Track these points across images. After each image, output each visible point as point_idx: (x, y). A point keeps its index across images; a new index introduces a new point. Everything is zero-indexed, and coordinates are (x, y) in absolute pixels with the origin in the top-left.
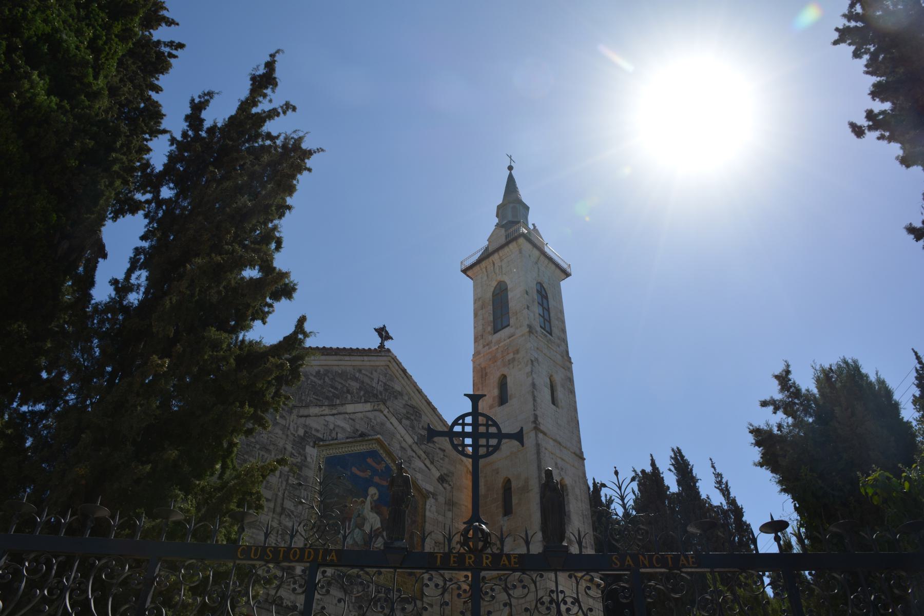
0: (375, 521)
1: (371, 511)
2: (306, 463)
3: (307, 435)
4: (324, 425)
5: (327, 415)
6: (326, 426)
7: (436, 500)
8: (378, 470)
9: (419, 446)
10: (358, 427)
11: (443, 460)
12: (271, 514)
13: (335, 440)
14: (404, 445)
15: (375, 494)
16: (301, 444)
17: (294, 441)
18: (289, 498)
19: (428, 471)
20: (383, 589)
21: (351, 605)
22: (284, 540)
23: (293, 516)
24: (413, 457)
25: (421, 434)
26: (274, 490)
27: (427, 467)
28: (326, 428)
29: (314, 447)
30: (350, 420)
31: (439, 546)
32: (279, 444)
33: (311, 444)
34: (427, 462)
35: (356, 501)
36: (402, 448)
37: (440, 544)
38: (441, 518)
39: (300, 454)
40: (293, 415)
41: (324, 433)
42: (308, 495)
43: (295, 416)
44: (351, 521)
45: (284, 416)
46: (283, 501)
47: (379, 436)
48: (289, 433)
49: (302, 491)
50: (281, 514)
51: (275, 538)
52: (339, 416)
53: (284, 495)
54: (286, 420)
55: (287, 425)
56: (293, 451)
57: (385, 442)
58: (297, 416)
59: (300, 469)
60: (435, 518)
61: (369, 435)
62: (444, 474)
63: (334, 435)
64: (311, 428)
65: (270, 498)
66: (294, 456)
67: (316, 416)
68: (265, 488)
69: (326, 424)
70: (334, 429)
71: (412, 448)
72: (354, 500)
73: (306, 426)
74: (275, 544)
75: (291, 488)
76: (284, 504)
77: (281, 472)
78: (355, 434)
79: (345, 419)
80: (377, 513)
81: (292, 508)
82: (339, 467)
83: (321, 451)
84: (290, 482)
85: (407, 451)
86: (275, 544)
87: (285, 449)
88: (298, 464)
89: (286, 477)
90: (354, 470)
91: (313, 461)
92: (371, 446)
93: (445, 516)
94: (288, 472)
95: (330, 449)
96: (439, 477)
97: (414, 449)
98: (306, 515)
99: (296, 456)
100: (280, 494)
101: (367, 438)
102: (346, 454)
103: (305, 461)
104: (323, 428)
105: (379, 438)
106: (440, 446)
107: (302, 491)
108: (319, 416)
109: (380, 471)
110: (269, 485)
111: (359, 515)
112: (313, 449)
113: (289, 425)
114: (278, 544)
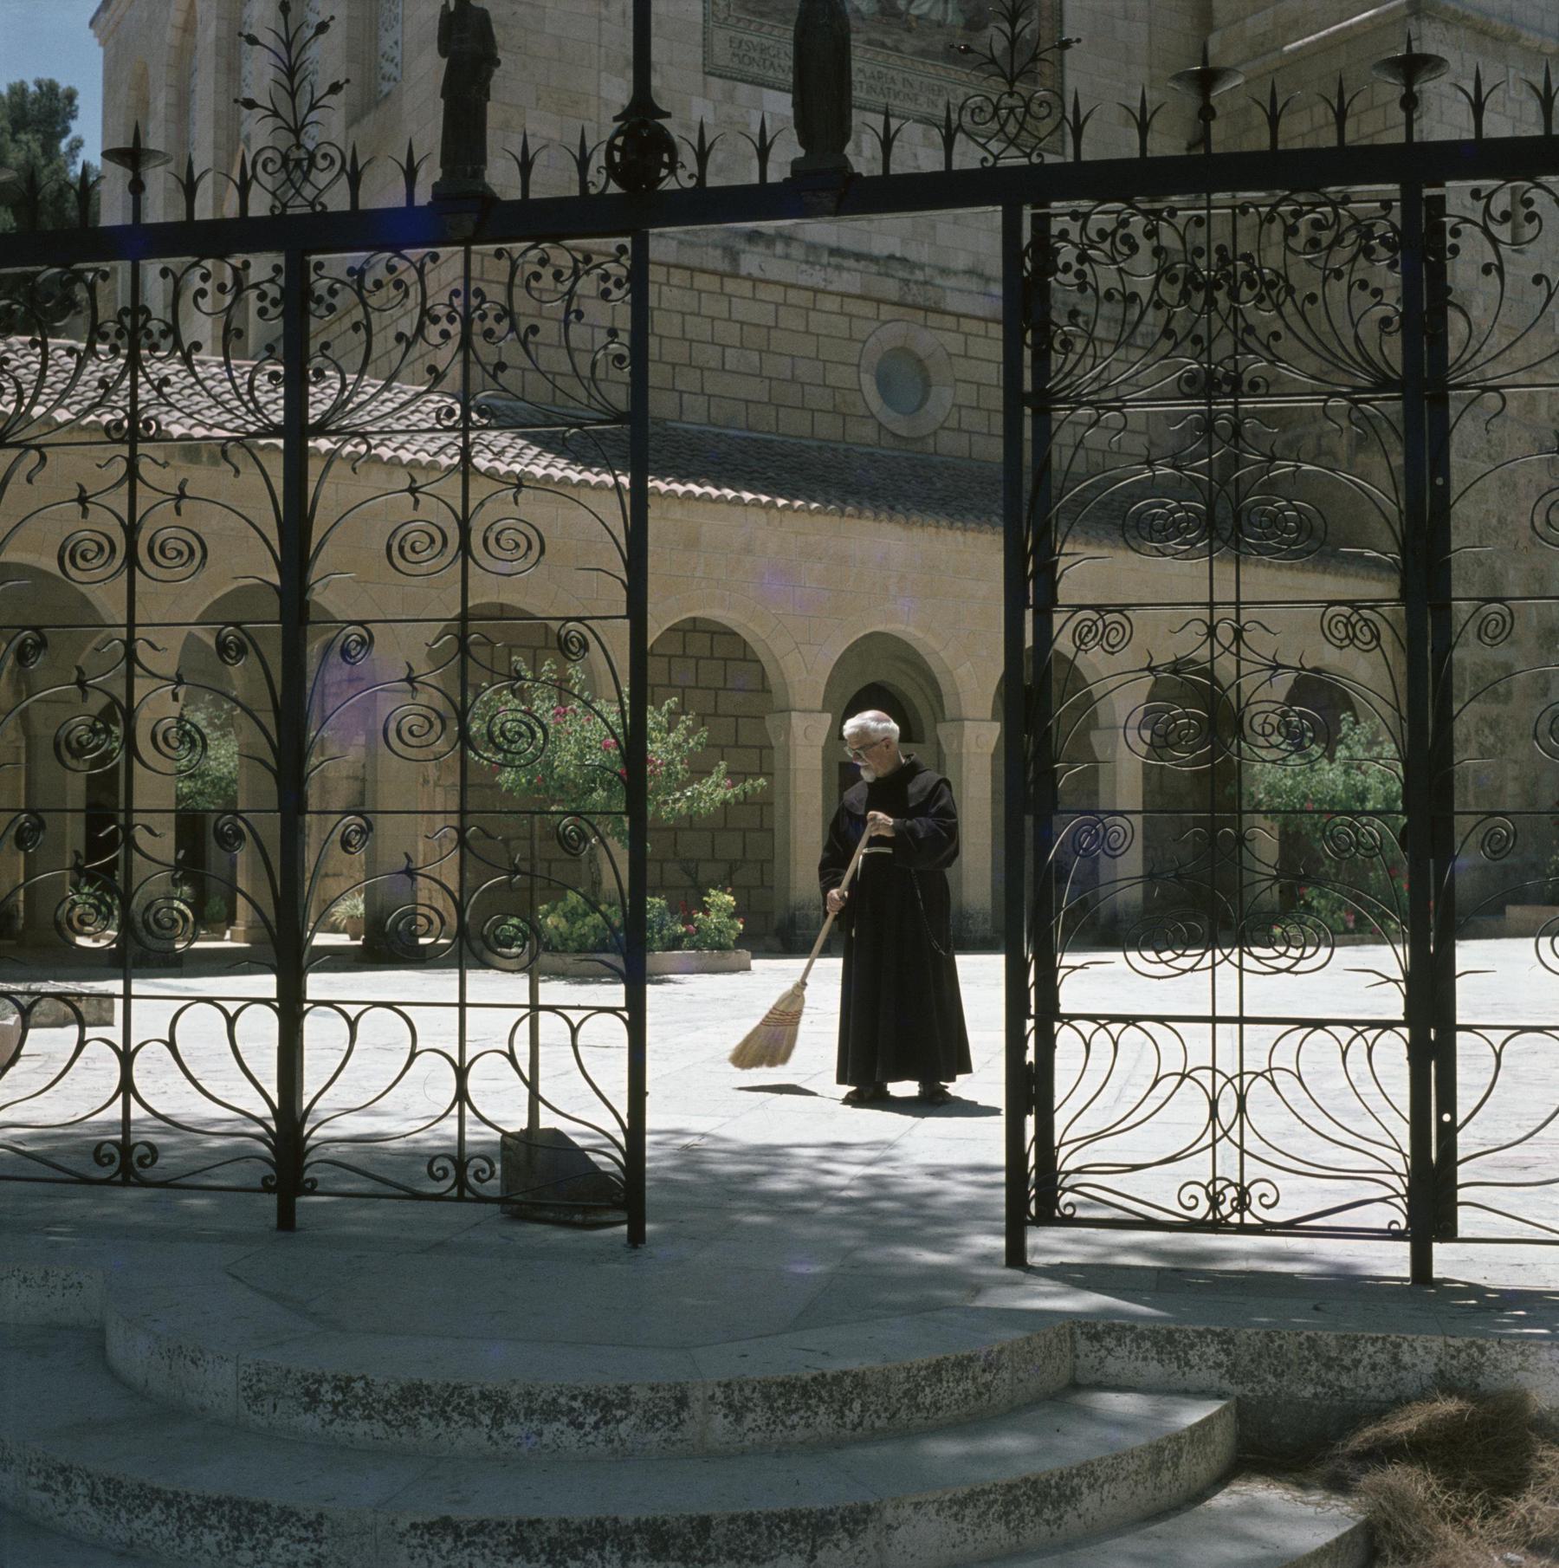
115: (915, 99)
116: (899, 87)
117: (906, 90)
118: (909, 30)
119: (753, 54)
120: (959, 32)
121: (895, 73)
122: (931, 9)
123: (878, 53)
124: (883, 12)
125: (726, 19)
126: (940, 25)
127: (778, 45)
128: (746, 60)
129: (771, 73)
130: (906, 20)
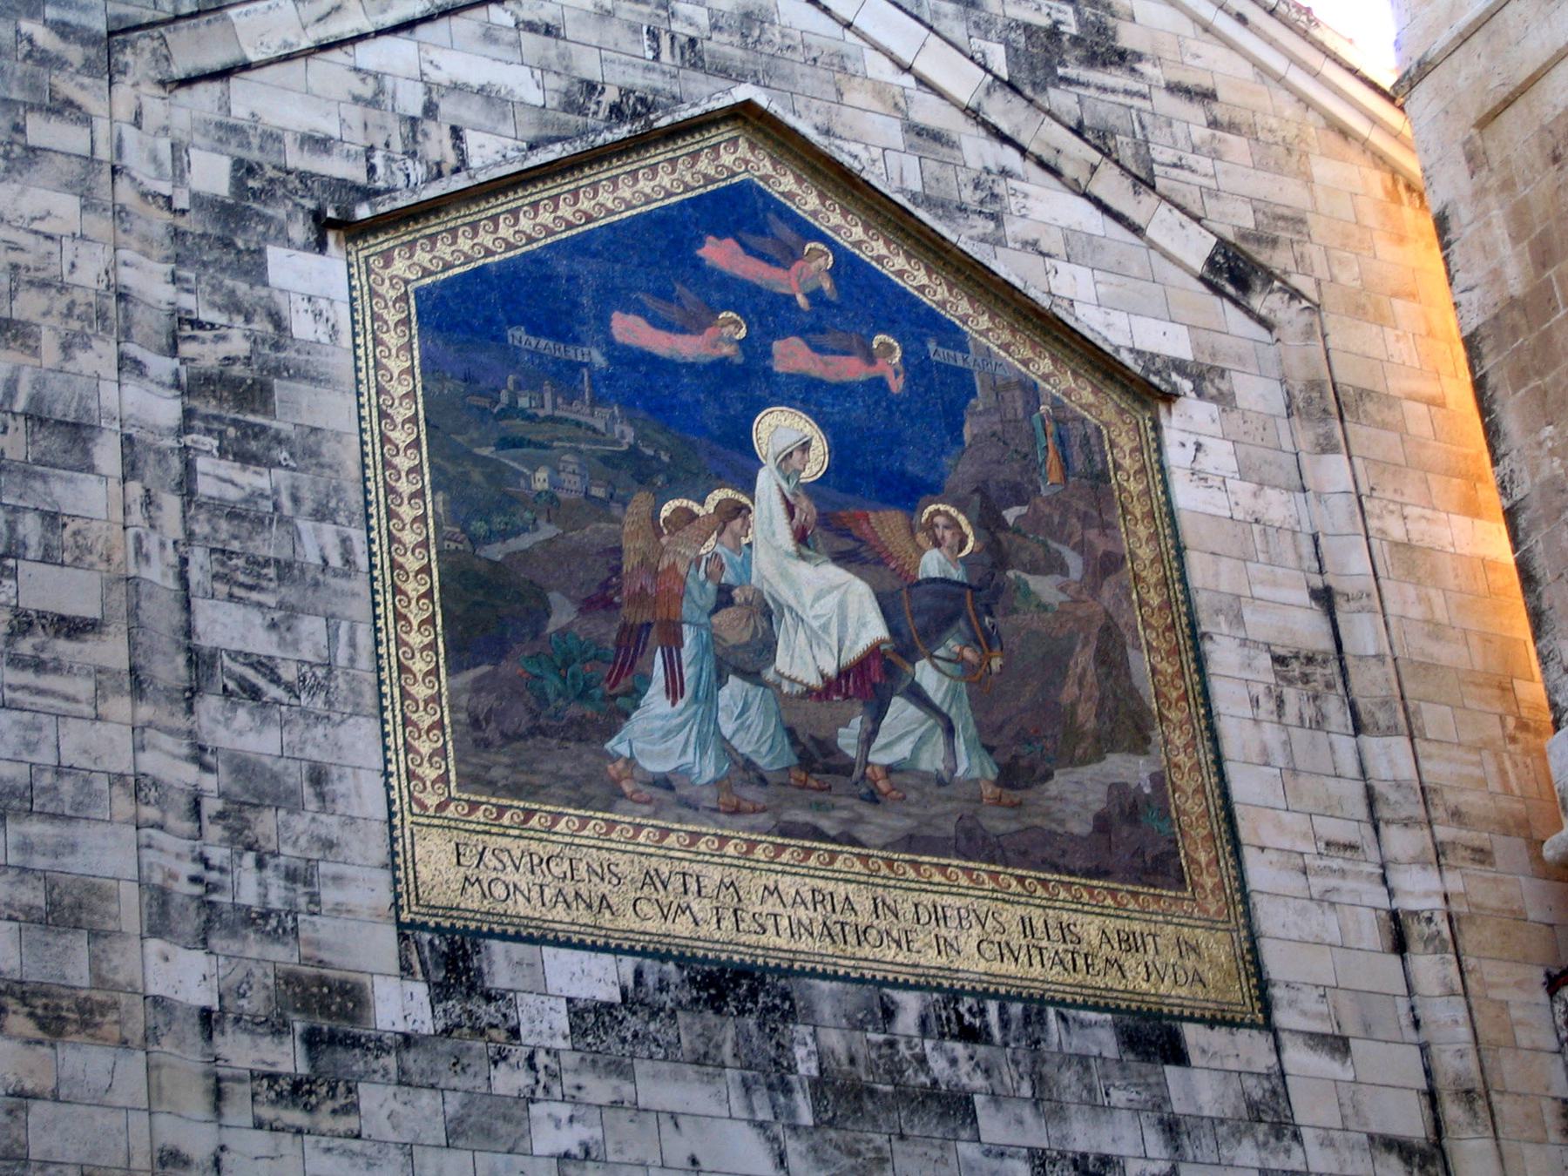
0: (842, 606)
1: (802, 557)
2: (289, 354)
3: (251, 183)
4: (357, 99)
5: (362, 37)
6: (373, 102)
7: (1225, 400)
8: (791, 299)
9: (1031, 101)
10: (589, 66)
11: (1216, 155)
12: (120, 707)
13: (456, 171)
14: (929, 112)
15: (805, 446)
16: (228, 244)
17: (177, 235)
18: (222, 588)
19: (1130, 237)
20: (992, 1007)
21: (794, 1147)
22: (249, 848)
23: (274, 692)
24: (1005, 173)
25: (1028, 28)
26: (108, 560)
27: (1118, 217)
28: (373, 114)
29: (321, 246)
30: (528, 38)
31: (1306, 679)
32: (77, 278)
33: (300, 230)
34: (1111, 186)
35: (693, 516)
36: (925, 136)
37: (1310, 660)
38: (1278, 506)
39: (233, 306)
40: (129, 80)
41: (372, 148)
42: (345, 541)
43: (148, 89)
44: (680, 644)
45: (69, 103)
46: (187, 606)
47: (742, 93)
48: (126, 193)
49: (305, 526)
50: (191, 696)
51: (185, 845)
52: (443, 24)
53: (183, 578)
54: (87, 120)
55: (104, 152)
56: (187, 301)
57: (790, 120)
58: (162, 83)
59: (254, 394)
60: (1238, 515)
61: (678, 100)
62: (1244, 236)
63: (438, 145)
64: (273, 138)
65: (91, 610)
66: (198, 324)
67: (288, 58)
68: (47, 558)
69: (367, 91)
70: (430, 110)
71: (985, 124)
72: (666, 511)
73: (235, 129)
74: (195, 880)
75: (224, 525)
76: (200, 624)
77: (128, 440)
78: (582, 111)
79: (489, 35)
80: (843, 559)
81: (262, 643)
82: (518, 336)
83: (376, 263)
84: (206, 487)
85: (952, 145)
86: (195, 880)
87: (122, 296)
88: (237, 370)
89: (176, 464)
90: (629, 329)
91: (334, 331)
92: (704, 165)
93: (1304, 490)
94: (185, 428)
95: (432, 238)
96: (1211, 261)
97: (1005, 127)
98: (365, 662)
99: (213, 326)
100: (159, 573)
101: (664, 122)
102: (547, 247)
103: (277, 346)
104: (357, 123)
105: (748, 105)
106: (1177, 76)
107: (305, 526)
108: (307, 53)
109: (801, 300)
110: (67, 533)
111: (725, 597)
112: (312, 260)
113: (119, 150)
114: (213, 876)
115: (904, 942)
116: (864, 919)
117: (883, 925)
118: (873, 798)
119: (511, 876)
120: (989, 791)
121: (851, 887)
122: (916, 750)
123: (809, 852)
124: (806, 761)
125: (441, 807)
126: (941, 782)
127: (568, 852)
128: (499, 891)
129: (560, 912)
130: (864, 777)
